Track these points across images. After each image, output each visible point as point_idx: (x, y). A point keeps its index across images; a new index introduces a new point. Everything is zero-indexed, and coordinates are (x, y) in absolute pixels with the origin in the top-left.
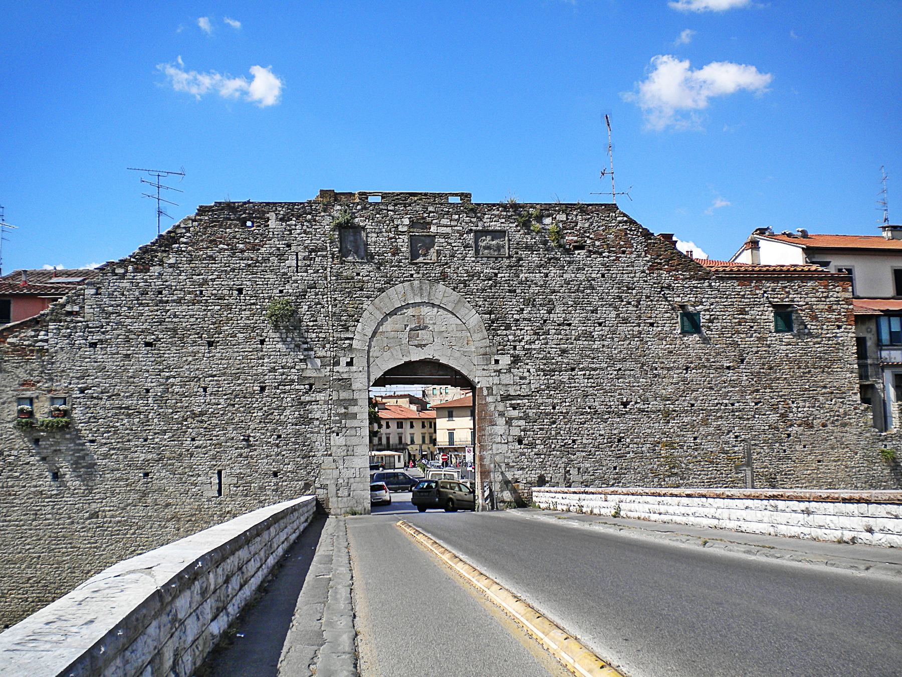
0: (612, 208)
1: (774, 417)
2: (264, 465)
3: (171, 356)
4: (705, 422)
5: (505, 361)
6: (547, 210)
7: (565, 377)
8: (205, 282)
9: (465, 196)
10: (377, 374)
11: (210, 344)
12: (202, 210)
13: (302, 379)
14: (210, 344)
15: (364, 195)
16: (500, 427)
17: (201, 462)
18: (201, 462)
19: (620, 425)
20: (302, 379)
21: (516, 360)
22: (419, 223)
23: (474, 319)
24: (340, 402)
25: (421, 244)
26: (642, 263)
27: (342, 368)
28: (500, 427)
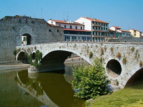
0: (44, 19)
1: (56, 40)
2: (12, 43)
3: (3, 32)
4: (51, 40)
5: (34, 34)
6: (38, 19)
7: (39, 36)
8: (6, 24)
9: (31, 17)
10: (22, 35)
11: (7, 31)
12: (6, 17)
13: (15, 35)
14: (7, 31)
15: (21, 16)
16: (33, 40)
17: (6, 43)
18: (6, 43)
19: (44, 40)
20: (15, 35)
21: (35, 34)
22: (26, 19)
23: (31, 30)
24: (19, 37)
25: (27, 22)
26: (46, 25)
27: (19, 34)
28: (33, 40)
